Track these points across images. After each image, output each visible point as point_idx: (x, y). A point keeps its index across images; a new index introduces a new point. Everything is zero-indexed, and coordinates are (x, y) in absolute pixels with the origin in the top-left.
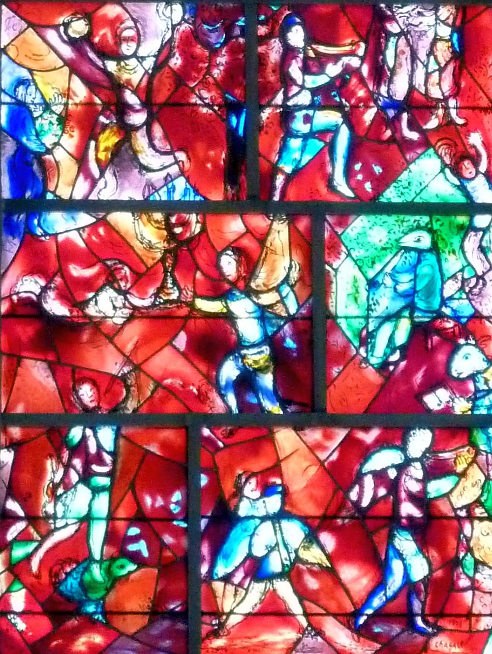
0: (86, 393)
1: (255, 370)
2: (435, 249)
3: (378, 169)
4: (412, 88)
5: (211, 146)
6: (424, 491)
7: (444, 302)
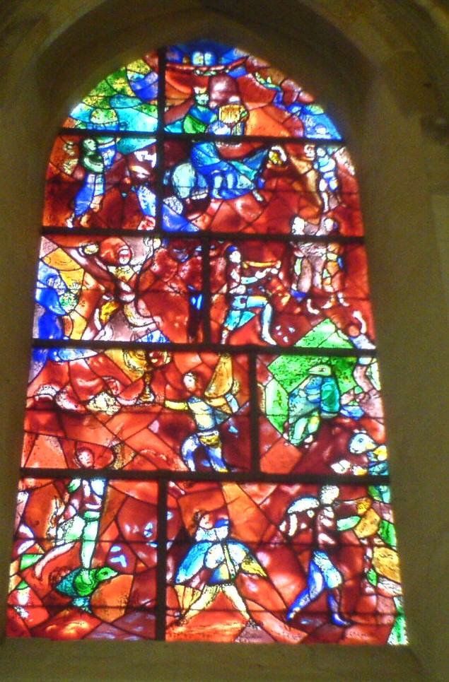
0: (85, 458)
1: (208, 446)
2: (333, 376)
3: (291, 330)
4: (313, 286)
5: (177, 314)
6: (335, 526)
7: (342, 407)
